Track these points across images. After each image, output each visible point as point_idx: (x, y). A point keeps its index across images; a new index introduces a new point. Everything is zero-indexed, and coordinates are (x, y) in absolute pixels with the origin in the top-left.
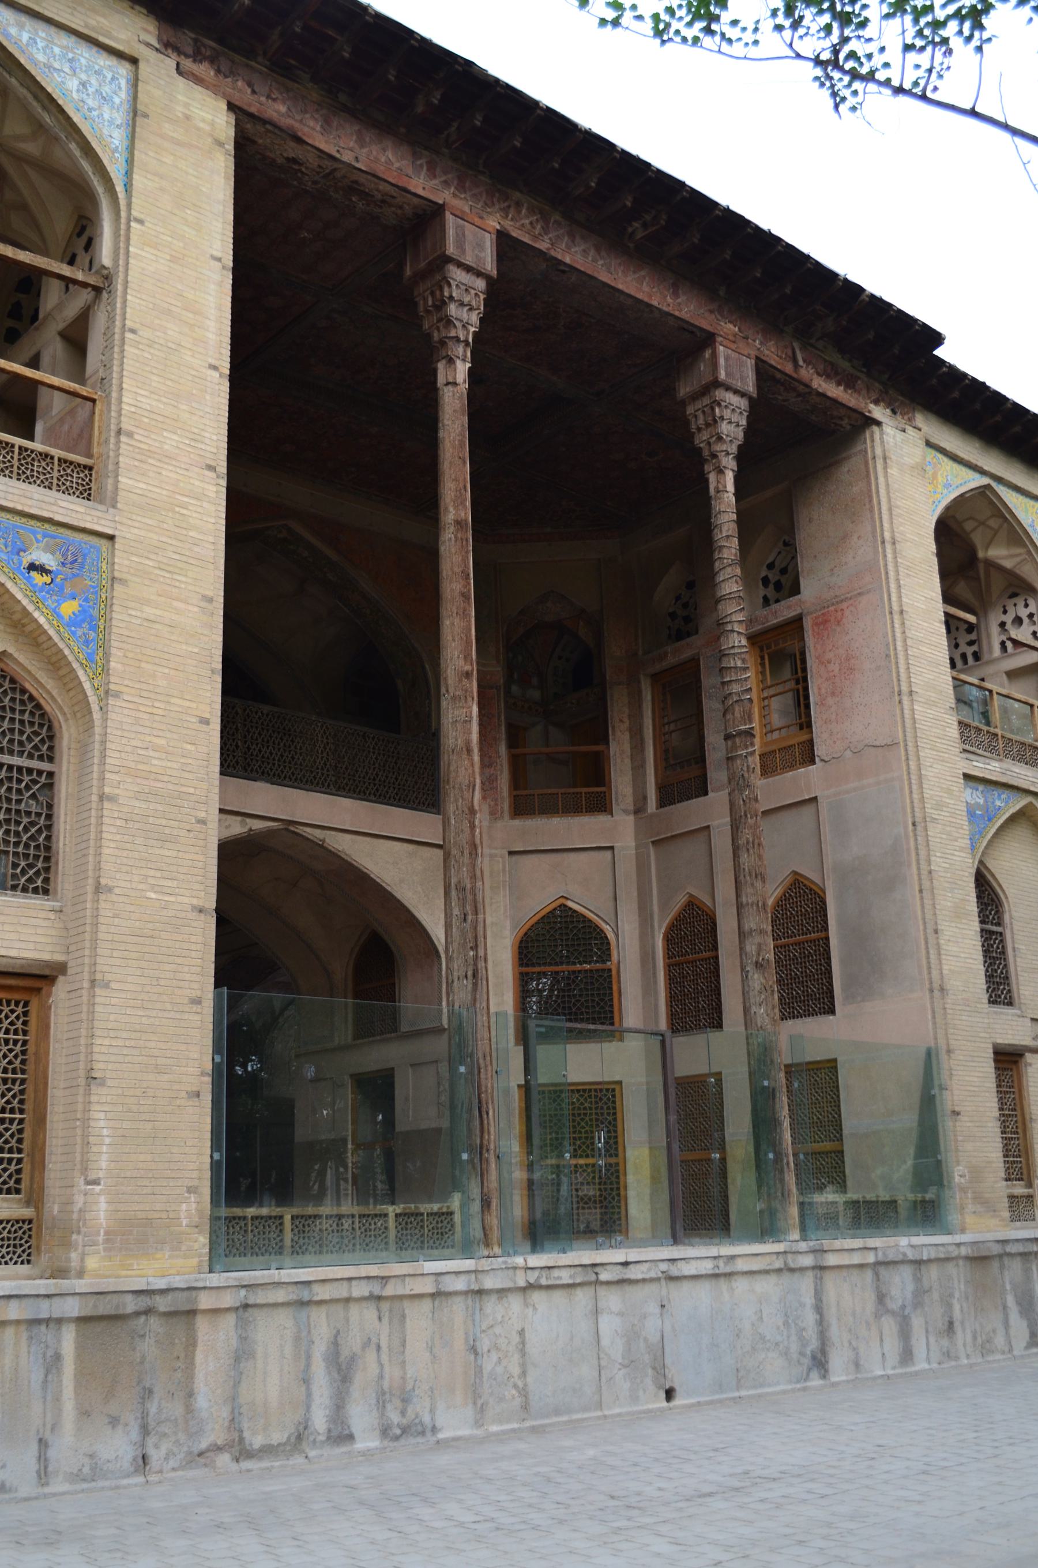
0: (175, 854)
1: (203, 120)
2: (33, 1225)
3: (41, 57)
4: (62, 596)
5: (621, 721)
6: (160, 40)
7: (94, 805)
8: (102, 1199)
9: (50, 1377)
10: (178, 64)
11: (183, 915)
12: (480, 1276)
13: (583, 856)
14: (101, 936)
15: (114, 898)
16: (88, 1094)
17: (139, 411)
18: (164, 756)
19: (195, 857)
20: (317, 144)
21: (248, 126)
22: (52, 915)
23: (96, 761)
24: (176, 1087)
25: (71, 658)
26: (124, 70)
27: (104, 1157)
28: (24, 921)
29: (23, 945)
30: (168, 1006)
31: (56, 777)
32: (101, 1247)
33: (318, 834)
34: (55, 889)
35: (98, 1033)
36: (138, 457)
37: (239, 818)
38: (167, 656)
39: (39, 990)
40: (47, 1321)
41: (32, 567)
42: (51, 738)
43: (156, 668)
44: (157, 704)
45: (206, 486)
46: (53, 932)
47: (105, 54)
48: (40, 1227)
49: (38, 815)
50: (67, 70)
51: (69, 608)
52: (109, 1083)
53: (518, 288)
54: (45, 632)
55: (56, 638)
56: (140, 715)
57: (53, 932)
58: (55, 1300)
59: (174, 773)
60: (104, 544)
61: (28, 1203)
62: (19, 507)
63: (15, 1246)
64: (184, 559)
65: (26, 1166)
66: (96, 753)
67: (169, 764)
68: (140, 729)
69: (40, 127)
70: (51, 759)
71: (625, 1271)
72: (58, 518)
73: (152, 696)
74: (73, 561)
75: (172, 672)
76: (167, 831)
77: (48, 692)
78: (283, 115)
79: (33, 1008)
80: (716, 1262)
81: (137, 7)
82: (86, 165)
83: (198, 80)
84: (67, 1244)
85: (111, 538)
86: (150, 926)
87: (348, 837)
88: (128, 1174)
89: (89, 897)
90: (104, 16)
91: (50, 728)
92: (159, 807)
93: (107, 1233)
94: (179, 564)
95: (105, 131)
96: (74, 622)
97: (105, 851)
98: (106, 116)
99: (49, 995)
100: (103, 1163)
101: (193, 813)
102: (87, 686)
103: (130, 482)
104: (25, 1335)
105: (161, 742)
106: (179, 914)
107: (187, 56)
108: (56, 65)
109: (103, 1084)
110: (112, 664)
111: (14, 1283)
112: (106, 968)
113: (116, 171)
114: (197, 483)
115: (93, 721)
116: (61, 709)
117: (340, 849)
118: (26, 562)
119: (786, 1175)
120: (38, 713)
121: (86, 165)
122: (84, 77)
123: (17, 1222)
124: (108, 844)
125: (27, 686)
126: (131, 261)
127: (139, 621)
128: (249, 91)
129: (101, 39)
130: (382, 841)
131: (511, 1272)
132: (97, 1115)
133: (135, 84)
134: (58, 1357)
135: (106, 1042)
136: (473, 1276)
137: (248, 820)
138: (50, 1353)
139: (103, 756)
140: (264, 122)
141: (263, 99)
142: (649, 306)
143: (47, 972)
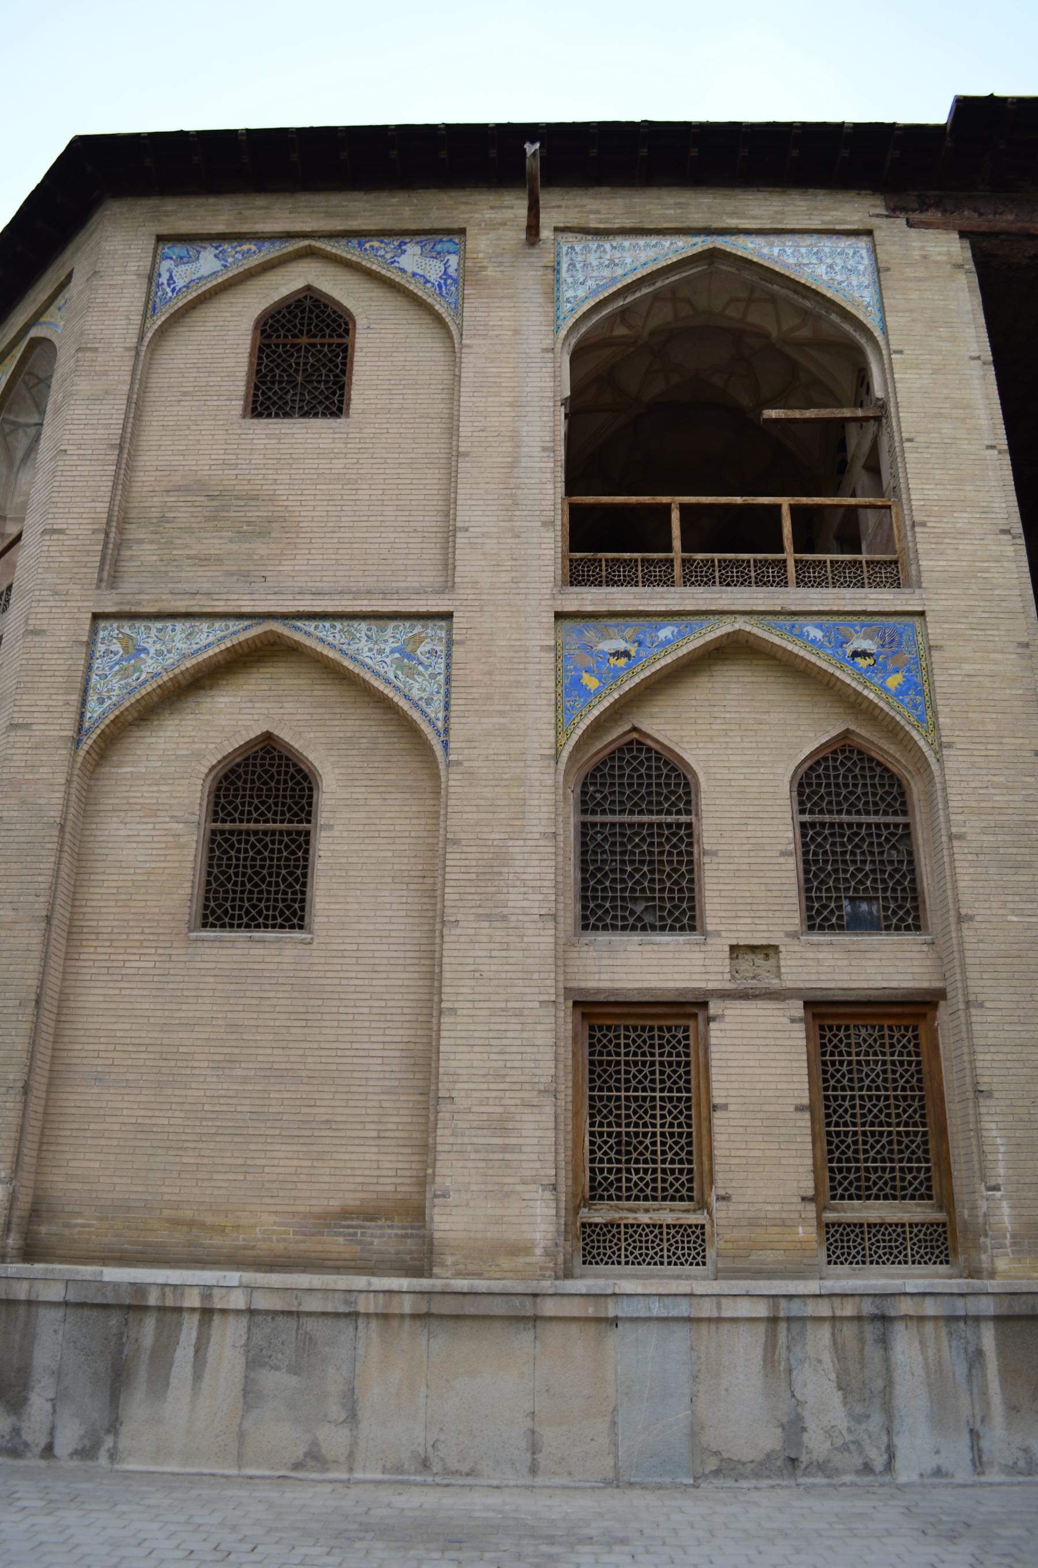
0: (1030, 878)
1: (940, 254)
2: (948, 1229)
3: (792, 261)
4: (887, 673)
6: (887, 208)
7: (945, 846)
8: (1004, 1204)
9: (974, 1371)
10: (907, 220)
14: (968, 961)
15: (977, 925)
16: (977, 1106)
18: (1005, 791)
21: (985, 244)
22: (925, 948)
23: (940, 806)
25: (903, 723)
26: (862, 244)
27: (1001, 1164)
28: (899, 955)
29: (901, 977)
31: (912, 827)
32: (1009, 1250)
34: (927, 927)
35: (979, 1049)
38: (992, 703)
39: (924, 1015)
40: (965, 1318)
41: (856, 654)
42: (902, 794)
43: (983, 715)
44: (990, 747)
45: (1003, 548)
46: (929, 963)
47: (844, 238)
48: (954, 1230)
49: (901, 862)
50: (814, 261)
51: (894, 681)
52: (996, 1095)
54: (876, 705)
55: (887, 709)
56: (976, 759)
57: (929, 963)
58: (970, 1299)
59: (1017, 805)
60: (917, 621)
61: (940, 1208)
62: (835, 608)
63: (932, 1247)
65: (934, 1174)
66: (940, 799)
68: (977, 771)
69: (806, 314)
70: (905, 813)
72: (870, 609)
73: (984, 740)
74: (891, 641)
76: (1019, 858)
77: (893, 756)
79: (922, 1031)
82: (847, 327)
83: (928, 225)
84: (979, 1248)
85: (922, 614)
86: (1016, 947)
88: (1028, 1180)
89: (953, 927)
90: (836, 210)
91: (900, 786)
92: (1007, 838)
93: (1013, 1236)
94: (990, 621)
95: (856, 295)
96: (901, 691)
97: (961, 884)
98: (855, 283)
99: (934, 1019)
100: (1000, 1171)
102: (922, 743)
103: (931, 563)
104: (944, 1331)
105: (1001, 779)
107: (914, 211)
108: (805, 261)
109: (989, 1095)
110: (941, 720)
111: (926, 1281)
112: (977, 990)
113: (871, 322)
114: (994, 548)
115: (932, 772)
116: (906, 768)
118: (849, 652)
120: (887, 775)
121: (847, 327)
122: (829, 261)
123: (932, 1225)
124: (962, 877)
125: (873, 754)
126: (898, 385)
127: (960, 678)
128: (976, 215)
129: (838, 227)
132: (988, 1126)
133: (873, 251)
134: (979, 1353)
135: (988, 1057)
138: (971, 1348)
139: (946, 801)
141: (991, 217)
143: (928, 999)
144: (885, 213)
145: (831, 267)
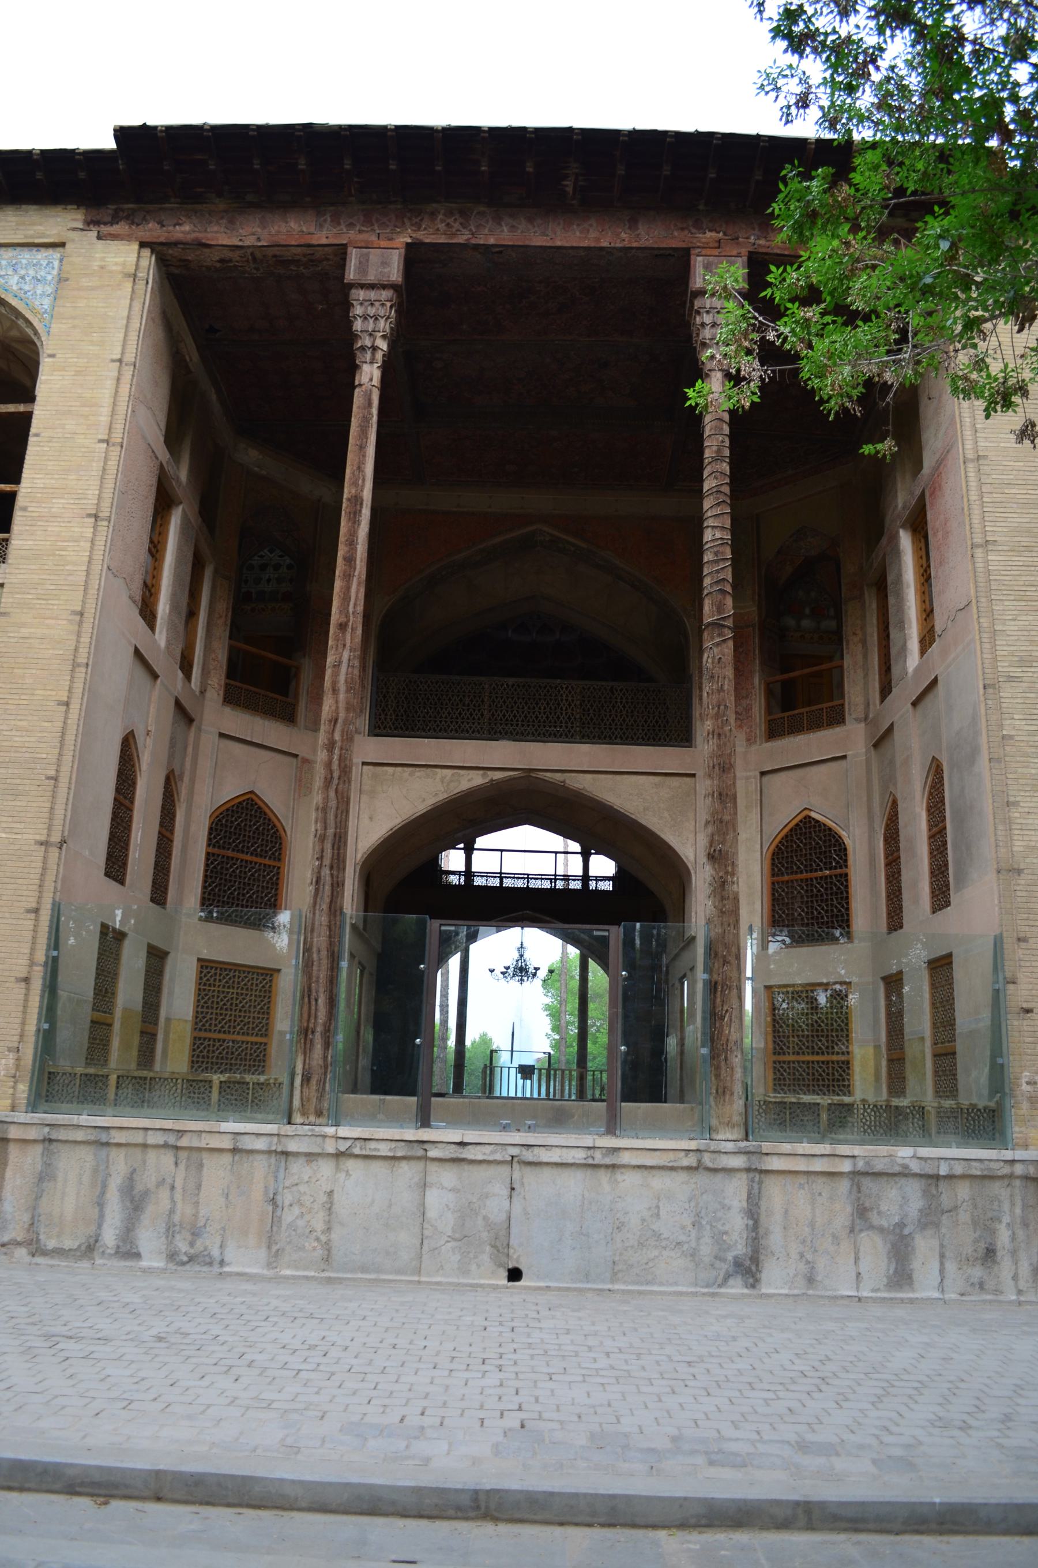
0: (24, 803)
5: (854, 634)
11: (27, 847)
12: (283, 1139)
13: (823, 768)
17: (34, 490)
19: (42, 804)
20: (220, 243)
24: (7, 974)
26: (55, 255)
30: (7, 915)
33: (558, 777)
36: (29, 523)
37: (481, 772)
38: (36, 661)
44: (23, 697)
50: (10, 272)
53: (425, 286)
56: (9, 707)
64: (59, 587)
67: (28, 739)
68: (7, 717)
71: (461, 1150)
73: (20, 691)
75: (38, 672)
78: (189, 233)
80: (589, 1153)
81: (69, 207)
83: (114, 237)
87: (589, 776)
90: (40, 225)
92: (16, 771)
94: (54, 592)
98: (39, 292)
101: (44, 772)
103: (21, 542)
105: (24, 723)
106: (24, 848)
107: (105, 224)
114: (76, 529)
117: (581, 787)
119: (723, 1072)
122: (23, 272)
127: (15, 640)
129: (37, 241)
130: (626, 776)
131: (319, 1139)
136: (275, 1139)
137: (489, 773)
140: (176, 244)
142: (602, 249)
144: (81, 227)
145: (23, 278)
